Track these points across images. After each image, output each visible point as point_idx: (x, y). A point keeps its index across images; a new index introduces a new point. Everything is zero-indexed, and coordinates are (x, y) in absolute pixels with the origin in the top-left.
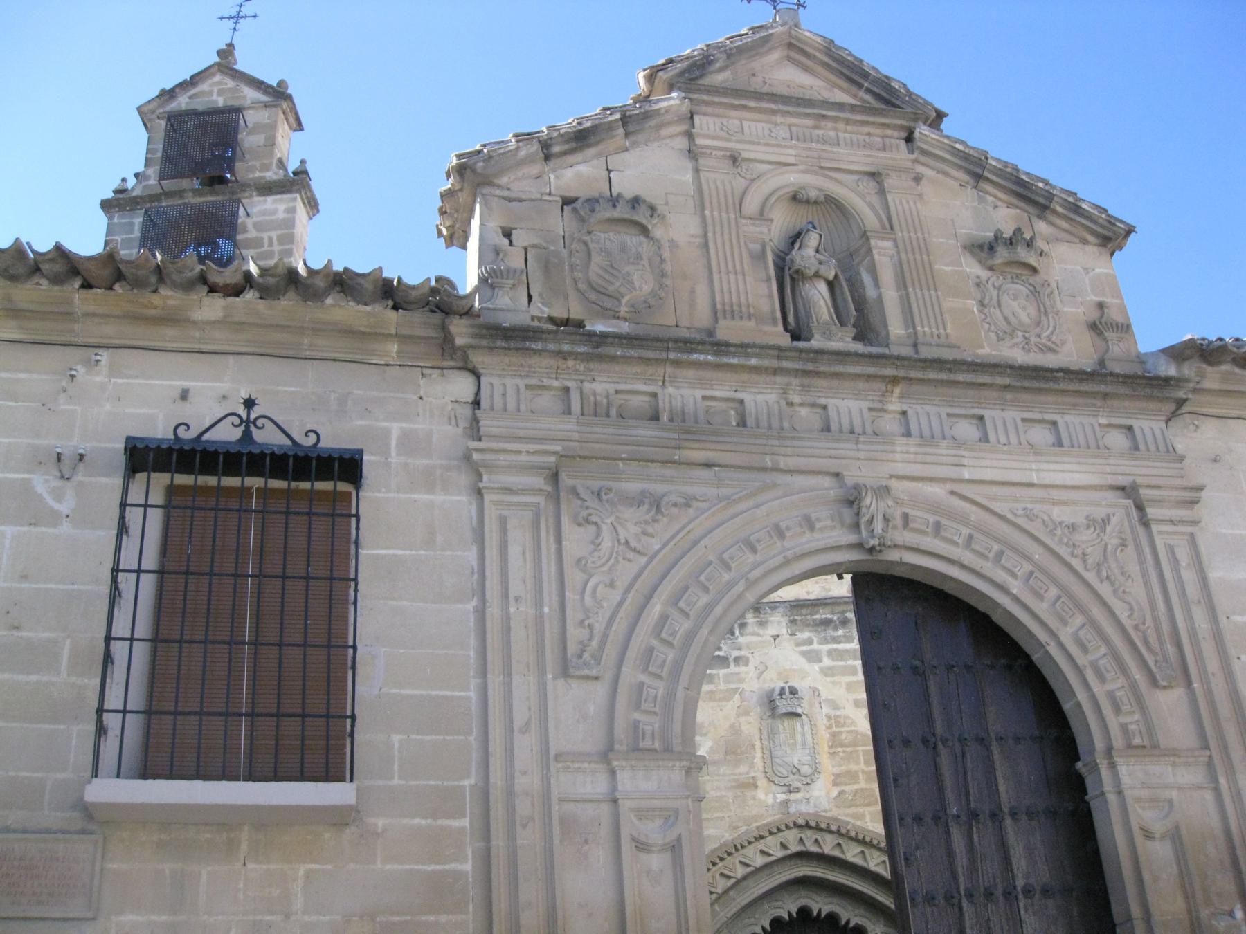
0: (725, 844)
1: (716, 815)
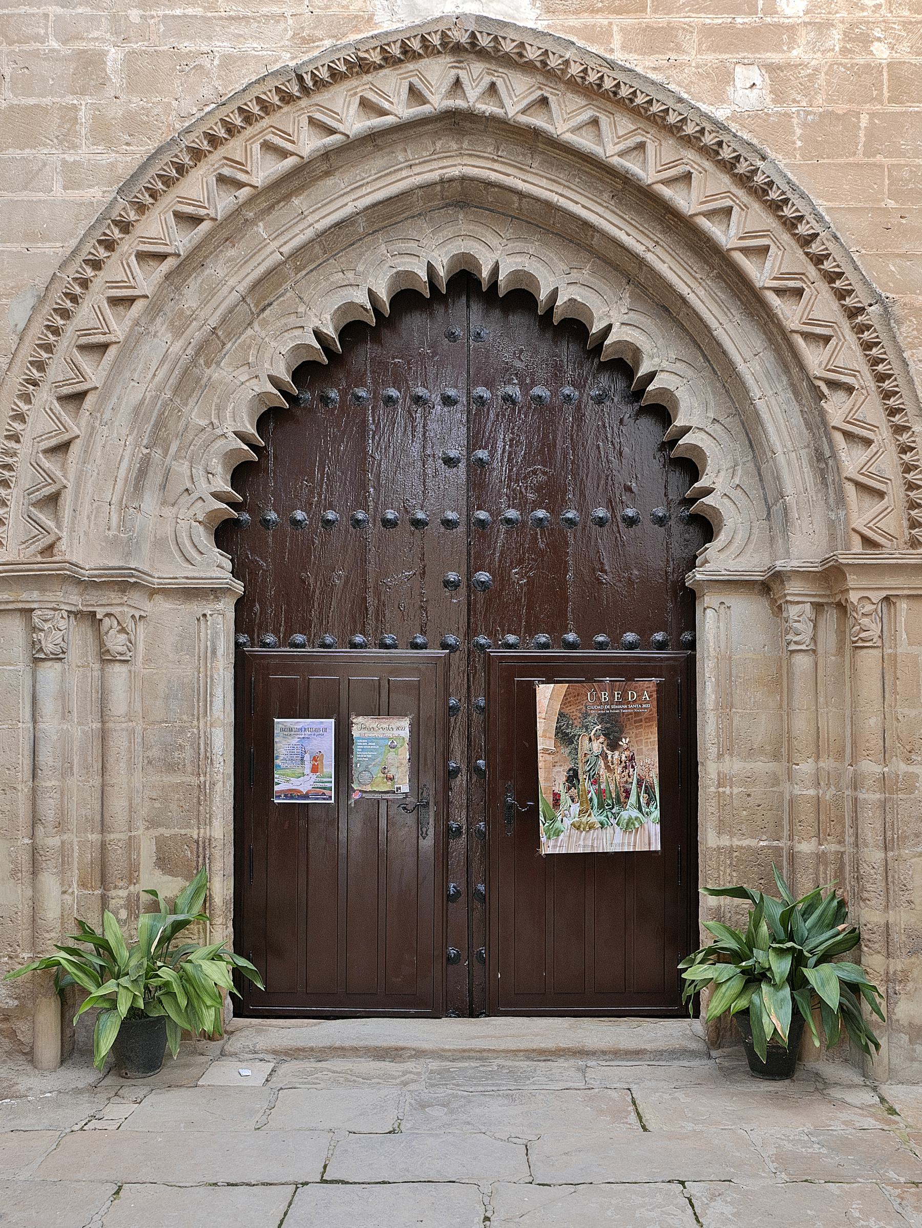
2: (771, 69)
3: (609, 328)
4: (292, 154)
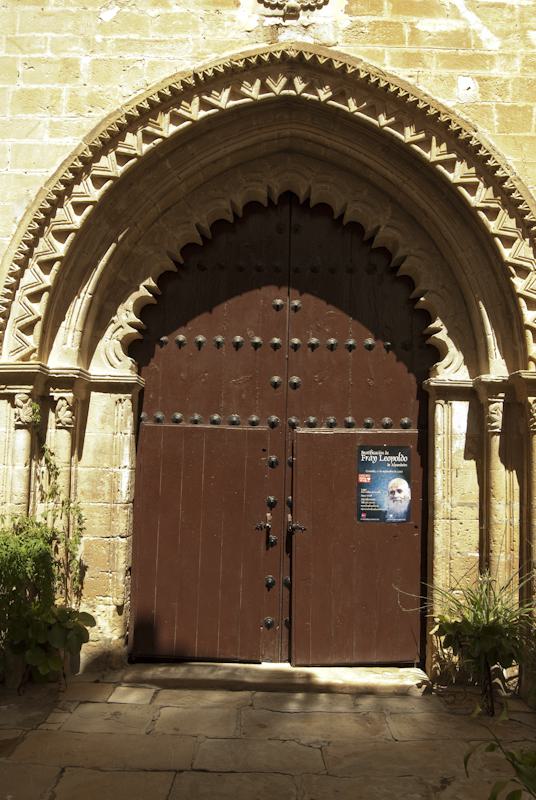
0: (181, 73)
1: (176, 37)
2: (480, 79)
3: (379, 227)
4: (189, 119)
